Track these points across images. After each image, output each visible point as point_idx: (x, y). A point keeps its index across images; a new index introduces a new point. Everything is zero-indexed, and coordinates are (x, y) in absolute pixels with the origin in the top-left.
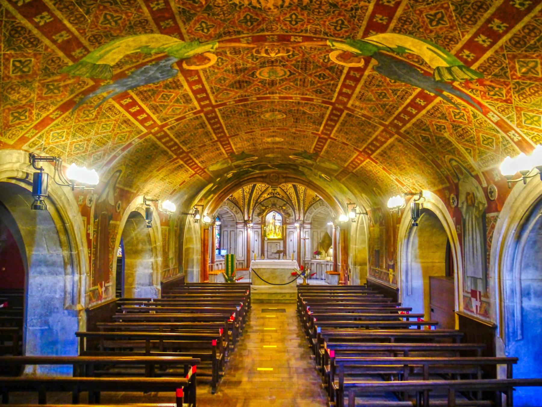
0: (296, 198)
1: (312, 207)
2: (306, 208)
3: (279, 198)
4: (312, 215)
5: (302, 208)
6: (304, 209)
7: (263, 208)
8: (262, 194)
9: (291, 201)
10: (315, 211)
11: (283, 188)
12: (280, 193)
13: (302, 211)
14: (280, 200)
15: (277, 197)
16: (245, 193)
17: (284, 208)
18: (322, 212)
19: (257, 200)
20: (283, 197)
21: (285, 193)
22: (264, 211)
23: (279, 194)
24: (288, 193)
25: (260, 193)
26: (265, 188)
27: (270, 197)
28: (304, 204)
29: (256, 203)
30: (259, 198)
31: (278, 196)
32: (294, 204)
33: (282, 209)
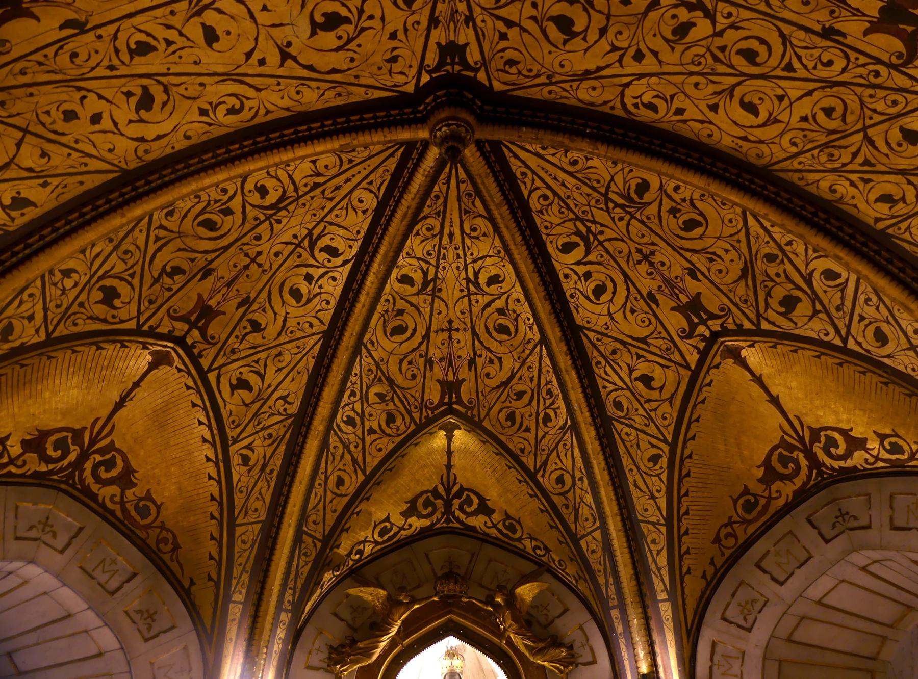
0: (610, 508)
1: (745, 568)
2: (693, 587)
3: (484, 539)
4: (761, 634)
5: (660, 586)
6: (676, 594)
7: (373, 595)
8: (361, 494)
9: (575, 539)
10: (787, 591)
11: (515, 444)
12: (493, 495)
13: (666, 610)
14: (490, 550)
15: (469, 532)
16: (238, 472)
17: (527, 592)
18: (844, 598)
19: (330, 540)
20: (512, 523)
21: (531, 476)
22: (378, 627)
23: (485, 509)
24: (548, 481)
25: (352, 482)
26: (387, 445)
27: (424, 534)
28: (675, 554)
29: (322, 563)
30: (340, 526)
31: (478, 522)
32: (596, 559)
33: (511, 600)
